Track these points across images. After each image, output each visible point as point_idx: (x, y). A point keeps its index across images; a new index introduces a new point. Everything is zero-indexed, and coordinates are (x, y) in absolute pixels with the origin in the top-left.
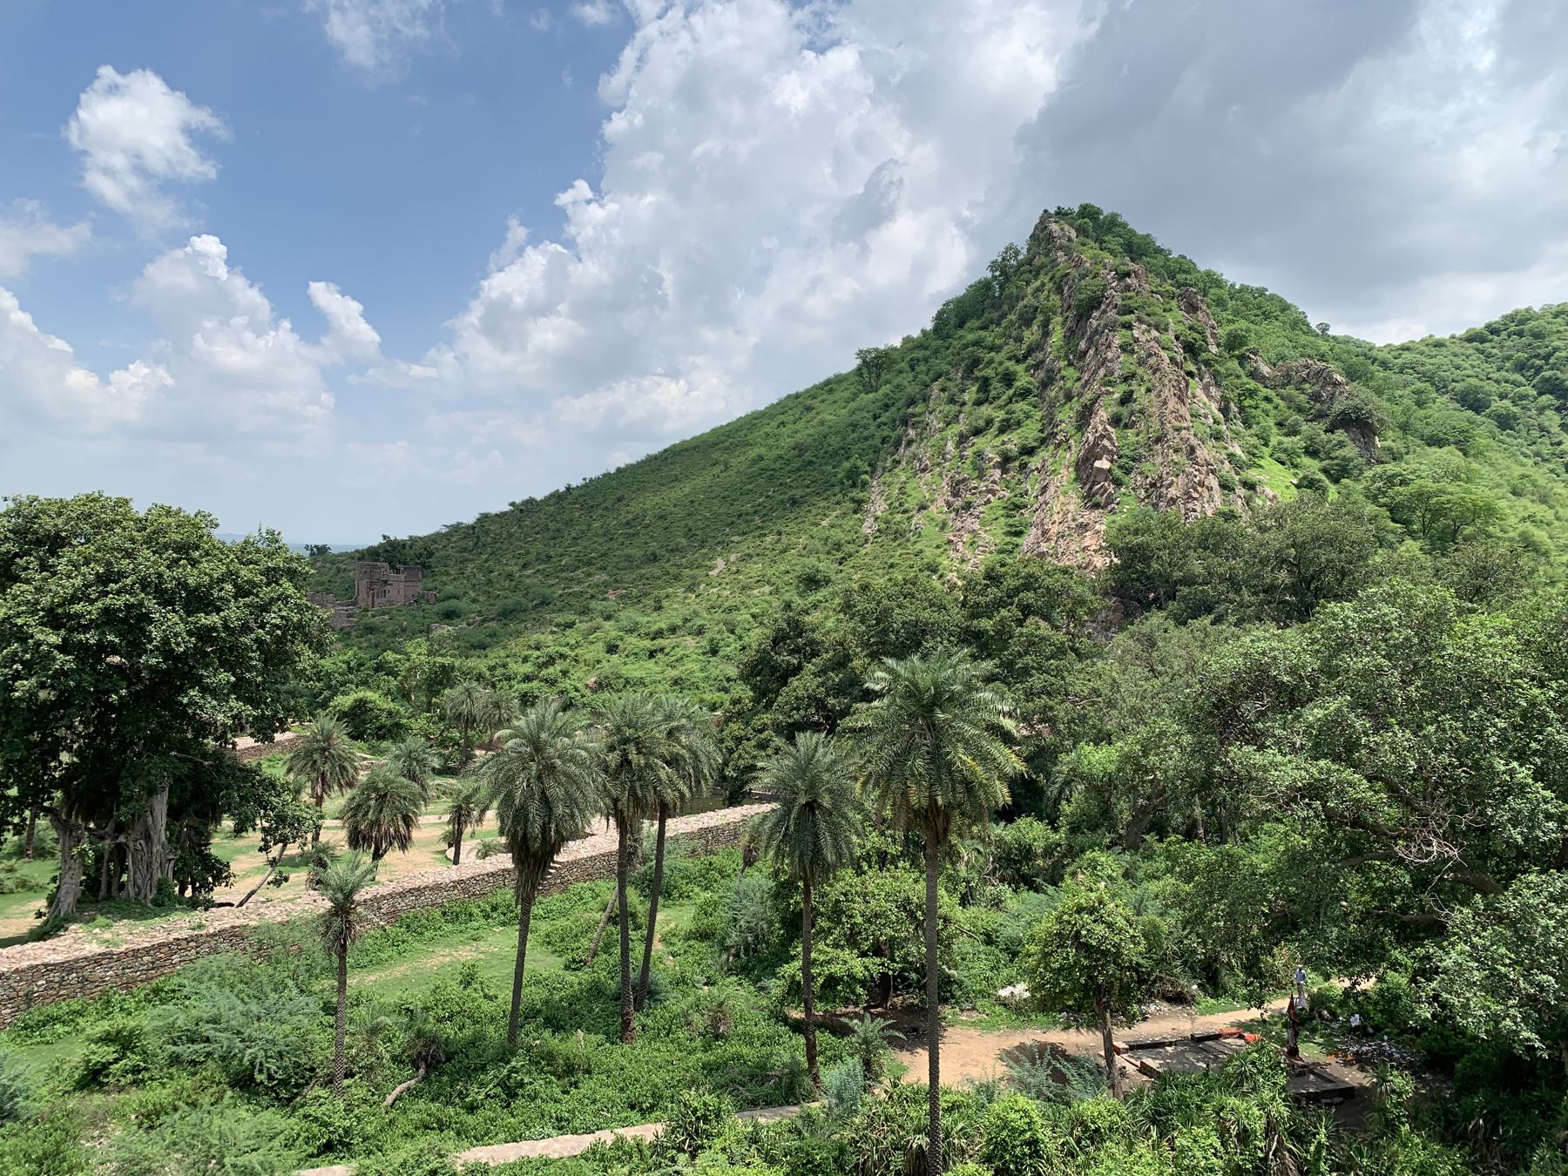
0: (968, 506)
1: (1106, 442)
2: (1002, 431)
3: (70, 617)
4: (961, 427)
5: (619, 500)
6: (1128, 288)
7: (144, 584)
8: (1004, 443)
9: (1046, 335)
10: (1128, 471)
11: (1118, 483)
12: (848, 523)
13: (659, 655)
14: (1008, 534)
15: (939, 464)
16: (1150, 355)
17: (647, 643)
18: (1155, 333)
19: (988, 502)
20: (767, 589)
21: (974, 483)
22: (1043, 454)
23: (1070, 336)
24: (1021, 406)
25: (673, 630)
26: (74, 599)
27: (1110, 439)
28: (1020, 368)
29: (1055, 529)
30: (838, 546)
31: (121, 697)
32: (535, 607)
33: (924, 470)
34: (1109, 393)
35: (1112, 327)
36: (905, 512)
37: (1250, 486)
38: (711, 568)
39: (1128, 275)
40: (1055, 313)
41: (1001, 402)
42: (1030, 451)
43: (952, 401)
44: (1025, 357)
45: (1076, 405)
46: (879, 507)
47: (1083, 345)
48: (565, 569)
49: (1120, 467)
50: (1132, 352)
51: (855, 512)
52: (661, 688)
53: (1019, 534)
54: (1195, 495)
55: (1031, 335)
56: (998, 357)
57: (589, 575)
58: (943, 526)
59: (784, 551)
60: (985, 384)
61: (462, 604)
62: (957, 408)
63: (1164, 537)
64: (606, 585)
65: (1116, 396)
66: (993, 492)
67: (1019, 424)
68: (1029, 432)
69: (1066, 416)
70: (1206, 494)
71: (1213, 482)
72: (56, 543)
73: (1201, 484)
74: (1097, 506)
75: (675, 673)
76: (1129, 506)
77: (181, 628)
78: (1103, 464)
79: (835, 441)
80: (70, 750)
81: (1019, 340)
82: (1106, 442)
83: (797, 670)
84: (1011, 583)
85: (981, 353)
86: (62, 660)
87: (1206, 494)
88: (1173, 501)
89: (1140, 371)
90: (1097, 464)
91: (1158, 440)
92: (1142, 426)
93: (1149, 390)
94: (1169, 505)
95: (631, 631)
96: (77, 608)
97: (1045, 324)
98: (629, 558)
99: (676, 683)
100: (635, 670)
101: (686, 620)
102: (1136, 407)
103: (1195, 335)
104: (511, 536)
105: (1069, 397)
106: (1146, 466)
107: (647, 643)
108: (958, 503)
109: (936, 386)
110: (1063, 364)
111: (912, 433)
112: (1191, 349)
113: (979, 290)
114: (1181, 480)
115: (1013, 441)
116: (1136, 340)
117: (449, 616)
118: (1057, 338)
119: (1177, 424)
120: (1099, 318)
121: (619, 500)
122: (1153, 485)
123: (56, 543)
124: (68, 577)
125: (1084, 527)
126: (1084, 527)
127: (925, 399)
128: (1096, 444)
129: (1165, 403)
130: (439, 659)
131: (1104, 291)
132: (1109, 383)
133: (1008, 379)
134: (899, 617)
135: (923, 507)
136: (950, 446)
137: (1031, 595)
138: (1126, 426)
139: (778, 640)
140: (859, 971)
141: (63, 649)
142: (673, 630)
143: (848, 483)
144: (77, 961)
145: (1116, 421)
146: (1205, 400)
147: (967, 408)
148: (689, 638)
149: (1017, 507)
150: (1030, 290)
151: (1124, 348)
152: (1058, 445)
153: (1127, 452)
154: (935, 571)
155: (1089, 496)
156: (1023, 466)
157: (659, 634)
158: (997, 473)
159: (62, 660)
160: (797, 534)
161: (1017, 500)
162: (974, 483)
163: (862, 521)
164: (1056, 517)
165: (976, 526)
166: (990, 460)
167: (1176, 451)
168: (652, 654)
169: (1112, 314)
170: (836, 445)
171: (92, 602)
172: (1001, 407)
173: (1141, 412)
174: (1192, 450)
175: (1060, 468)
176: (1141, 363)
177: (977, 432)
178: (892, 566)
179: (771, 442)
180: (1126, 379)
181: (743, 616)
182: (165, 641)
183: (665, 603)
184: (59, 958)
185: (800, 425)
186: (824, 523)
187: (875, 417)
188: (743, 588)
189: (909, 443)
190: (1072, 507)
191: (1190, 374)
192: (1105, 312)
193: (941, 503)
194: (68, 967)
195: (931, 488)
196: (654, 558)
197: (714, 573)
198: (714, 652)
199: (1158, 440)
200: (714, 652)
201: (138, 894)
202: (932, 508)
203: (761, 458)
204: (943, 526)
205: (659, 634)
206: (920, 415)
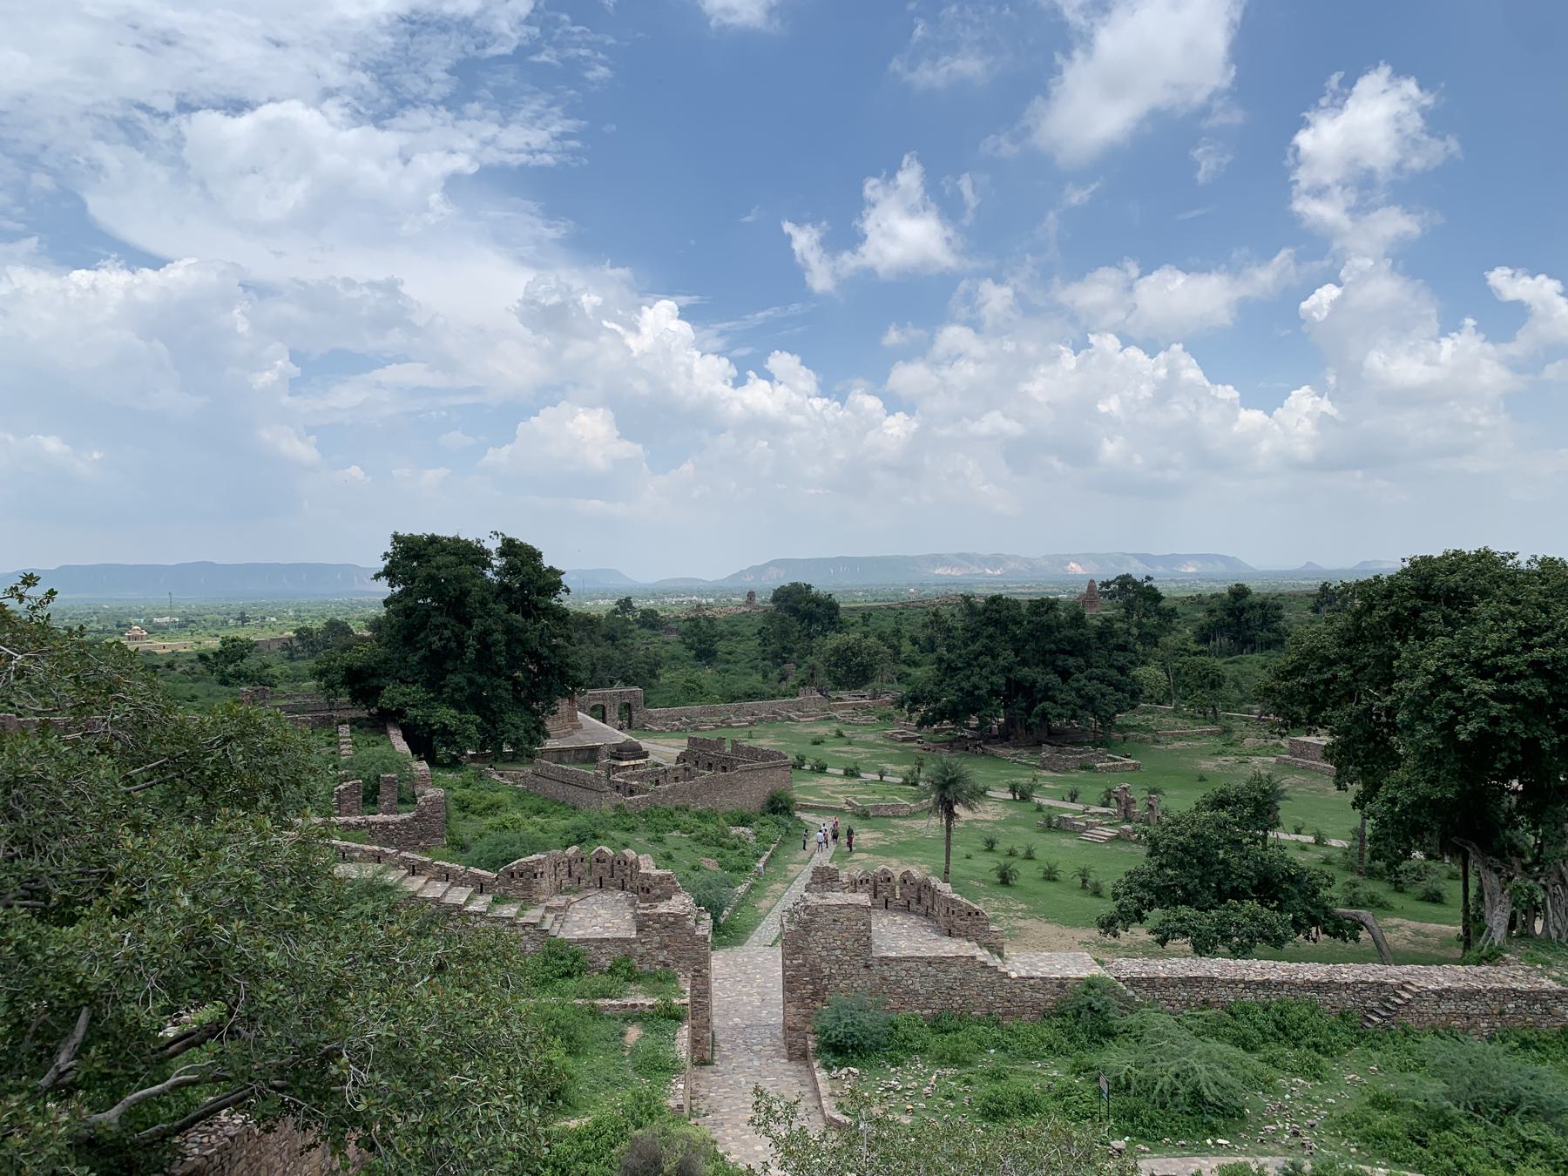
3: (1500, 669)
26: (1500, 652)
31: (1552, 745)
80: (1515, 792)
86: (1496, 708)
124: (1488, 632)
141: (1498, 697)
144: (1541, 992)
159: (1496, 708)
171: (1518, 655)
184: (1525, 986)
194: (1533, 997)
201: (1559, 936)
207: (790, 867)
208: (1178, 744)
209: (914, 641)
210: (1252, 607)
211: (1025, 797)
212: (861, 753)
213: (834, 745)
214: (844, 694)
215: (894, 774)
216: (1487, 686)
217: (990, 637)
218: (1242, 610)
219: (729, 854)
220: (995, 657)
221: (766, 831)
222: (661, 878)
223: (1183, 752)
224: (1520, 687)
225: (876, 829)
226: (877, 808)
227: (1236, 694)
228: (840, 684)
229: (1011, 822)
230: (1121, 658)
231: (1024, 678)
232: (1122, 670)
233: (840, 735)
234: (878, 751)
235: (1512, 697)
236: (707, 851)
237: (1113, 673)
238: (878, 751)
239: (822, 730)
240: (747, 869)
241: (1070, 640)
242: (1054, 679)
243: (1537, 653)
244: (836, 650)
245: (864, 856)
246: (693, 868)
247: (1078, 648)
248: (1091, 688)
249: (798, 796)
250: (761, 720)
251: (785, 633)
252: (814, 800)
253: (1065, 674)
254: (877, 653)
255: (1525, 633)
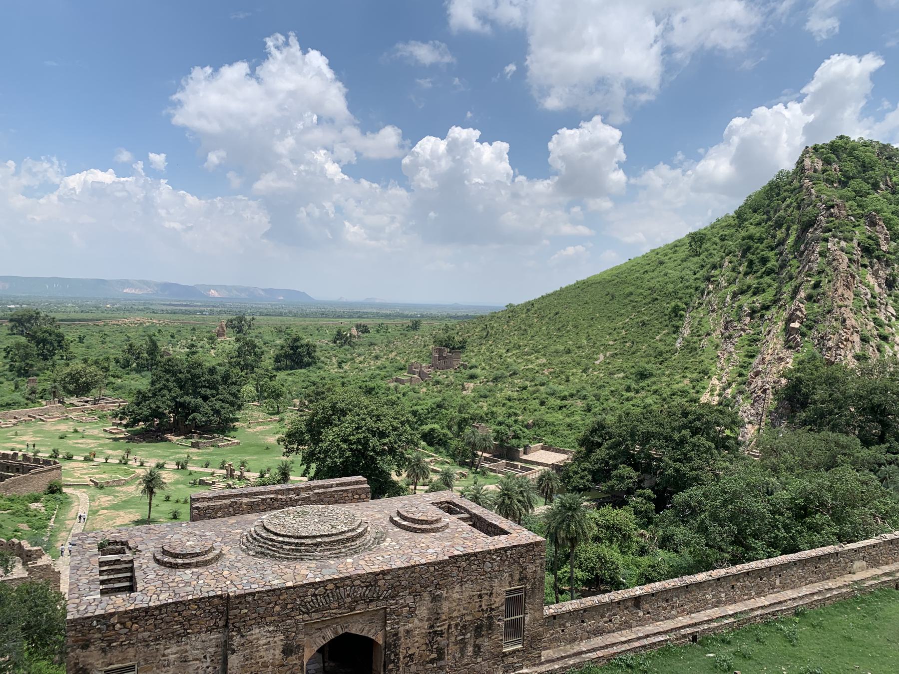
0: (730, 337)
1: (798, 313)
2: (754, 294)
4: (734, 288)
5: (557, 314)
6: (831, 215)
7: (368, 429)
8: (754, 302)
9: (788, 235)
10: (810, 328)
11: (803, 335)
12: (669, 340)
13: (564, 409)
14: (746, 356)
15: (721, 309)
16: (834, 260)
17: (558, 402)
18: (843, 244)
19: (741, 335)
20: (621, 375)
21: (735, 324)
22: (774, 310)
23: (799, 240)
24: (767, 279)
25: (572, 395)
27: (801, 311)
28: (771, 254)
29: (768, 358)
30: (661, 354)
32: (511, 375)
33: (713, 311)
34: (808, 281)
35: (817, 240)
36: (699, 336)
37: (885, 338)
38: (596, 359)
39: (833, 207)
40: (793, 223)
41: (759, 274)
42: (766, 308)
43: (734, 270)
44: (777, 246)
45: (794, 283)
46: (686, 332)
47: (802, 247)
48: (528, 354)
49: (806, 326)
50: (826, 256)
51: (674, 333)
52: (562, 428)
53: (752, 357)
54: (842, 346)
55: (780, 234)
56: (761, 246)
57: (537, 358)
58: (717, 347)
59: (633, 353)
60: (751, 263)
61: (478, 371)
62: (734, 274)
63: (812, 374)
64: (544, 365)
65: (812, 283)
66: (744, 330)
67: (764, 291)
68: (768, 296)
69: (787, 289)
70: (850, 345)
71: (856, 338)
72: (343, 413)
73: (847, 340)
74: (790, 347)
75: (568, 420)
76: (808, 348)
77: (378, 444)
78: (796, 325)
79: (670, 287)
81: (774, 236)
82: (798, 313)
83: (599, 445)
84: (690, 417)
85: (751, 243)
87: (850, 345)
88: (830, 349)
89: (827, 269)
90: (792, 325)
91: (829, 312)
92: (822, 302)
93: (829, 281)
94: (827, 351)
95: (553, 394)
96: (351, 438)
97: (788, 229)
98: (557, 352)
99: (569, 426)
100: (550, 418)
101: (578, 391)
102: (821, 290)
103: (871, 242)
104: (503, 331)
105: (791, 278)
106: (820, 327)
107: (558, 402)
108: (727, 334)
109: (727, 259)
110: (791, 257)
111: (711, 287)
112: (866, 251)
113: (766, 193)
114: (836, 337)
115: (759, 300)
116: (829, 249)
117: (472, 377)
118: (790, 241)
119: (840, 303)
120: (813, 233)
121: (557, 314)
122: (822, 338)
123: (343, 413)
125: (781, 359)
126: (781, 359)
127: (721, 266)
128: (792, 314)
129: (836, 290)
130: (463, 415)
131: (816, 217)
132: (809, 275)
133: (764, 261)
134: (641, 428)
135: (708, 334)
136: (728, 299)
137: (700, 423)
138: (814, 301)
139: (594, 431)
140: (580, 576)
142: (572, 395)
143: (673, 315)
145: (809, 298)
146: (872, 281)
147: (741, 276)
148: (579, 401)
149: (755, 341)
150: (784, 206)
151: (822, 254)
152: (780, 307)
153: (811, 317)
154: (706, 374)
155: (787, 342)
156: (762, 316)
157: (564, 398)
158: (747, 320)
159: (349, 454)
160: (642, 343)
161: (756, 337)
162: (735, 324)
163: (676, 339)
164: (770, 351)
165: (732, 350)
166: (745, 311)
167: (836, 320)
168: (560, 408)
169: (819, 233)
170: (671, 290)
172: (757, 278)
173: (823, 294)
174: (844, 320)
175: (777, 320)
176: (829, 263)
177: (742, 292)
178: (686, 368)
179: (638, 283)
180: (819, 273)
181: (605, 392)
182: (374, 447)
183: (571, 378)
185: (656, 273)
186: (657, 338)
187: (695, 274)
188: (610, 374)
189: (708, 293)
190: (778, 346)
191: (865, 266)
192: (816, 229)
193: (718, 332)
195: (714, 323)
196: (569, 352)
197: (597, 362)
198: (589, 410)
199: (829, 312)
200: (589, 410)
202: (714, 335)
203: (631, 294)
204: (717, 347)
205: (564, 398)
206: (717, 276)
207: (67, 522)
208: (259, 428)
209: (117, 361)
210: (302, 346)
211: (183, 468)
212: (91, 444)
213: (70, 439)
214: (74, 400)
215: (114, 457)
216: (345, 446)
217: (168, 380)
218: (298, 347)
219: (34, 520)
220: (170, 391)
221: (49, 504)
222: (36, 551)
223: (261, 433)
224: (354, 447)
225: (109, 495)
226: (108, 483)
227: (289, 396)
228: (71, 393)
229: (177, 482)
230: (234, 389)
231: (185, 402)
232: (234, 395)
233: (76, 431)
234: (101, 442)
235: (351, 450)
236: (20, 519)
237: (228, 396)
238: (101, 442)
239: (63, 427)
240: (46, 527)
241: (208, 381)
242: (200, 400)
243: (359, 436)
244: (69, 374)
245: (105, 511)
246: (16, 531)
247: (212, 386)
248: (218, 405)
249: (65, 479)
250: (21, 422)
251: (27, 356)
252: (71, 480)
253: (205, 398)
254: (96, 375)
255: (357, 428)
